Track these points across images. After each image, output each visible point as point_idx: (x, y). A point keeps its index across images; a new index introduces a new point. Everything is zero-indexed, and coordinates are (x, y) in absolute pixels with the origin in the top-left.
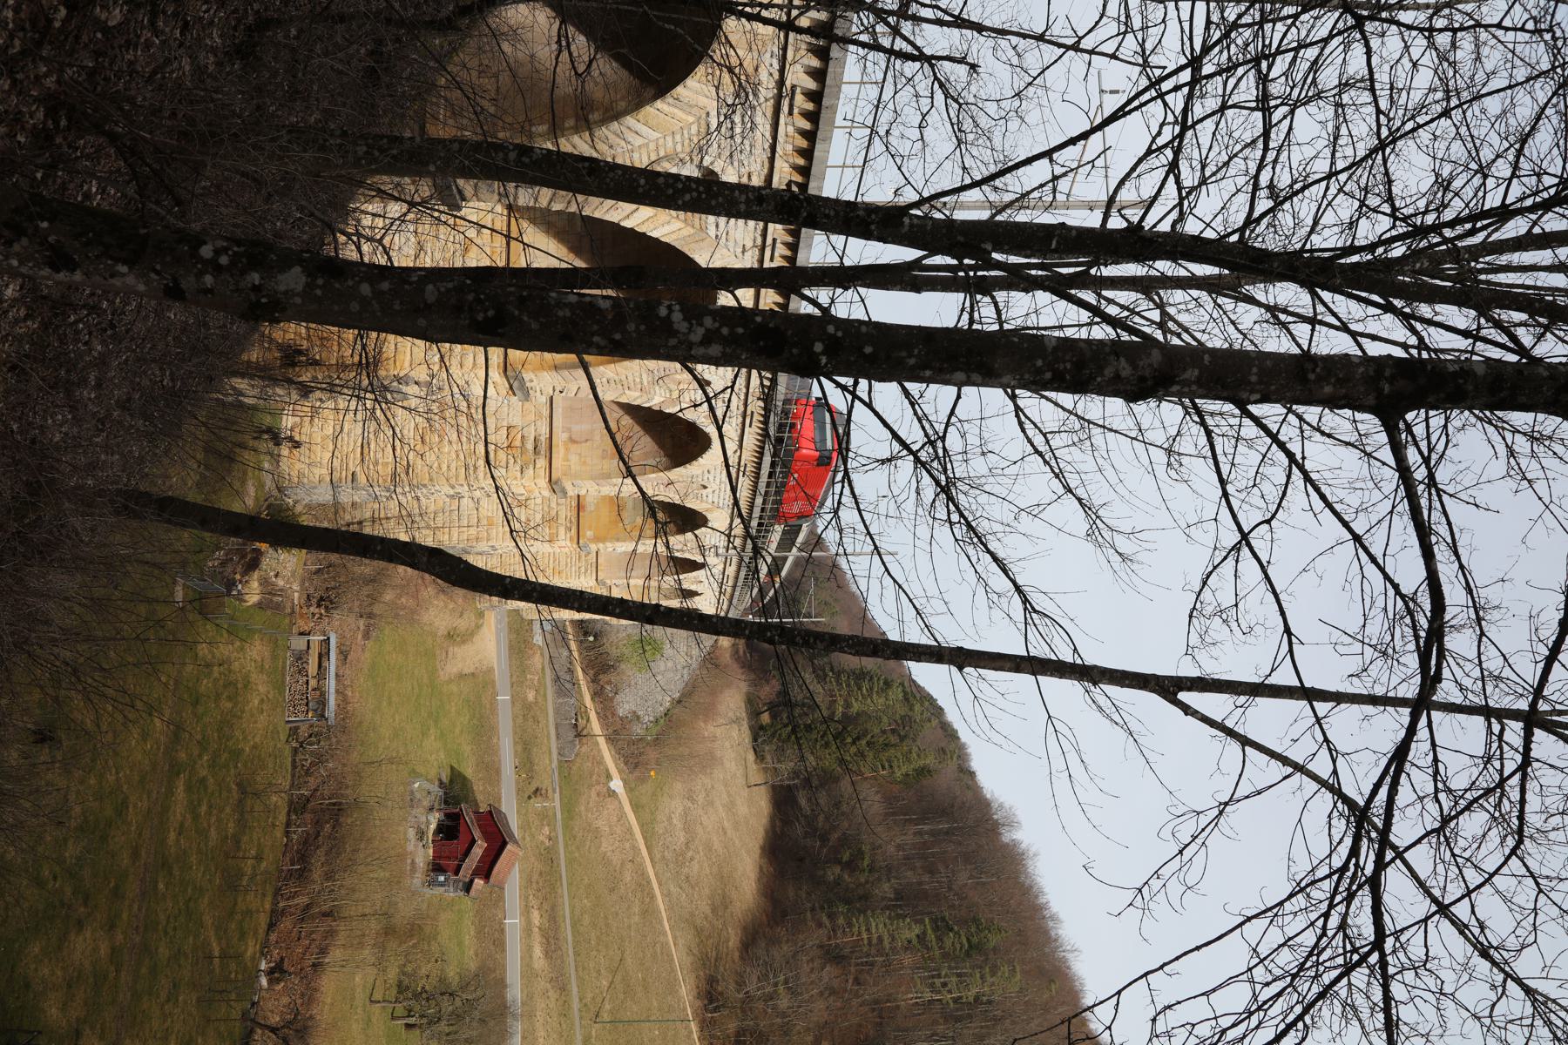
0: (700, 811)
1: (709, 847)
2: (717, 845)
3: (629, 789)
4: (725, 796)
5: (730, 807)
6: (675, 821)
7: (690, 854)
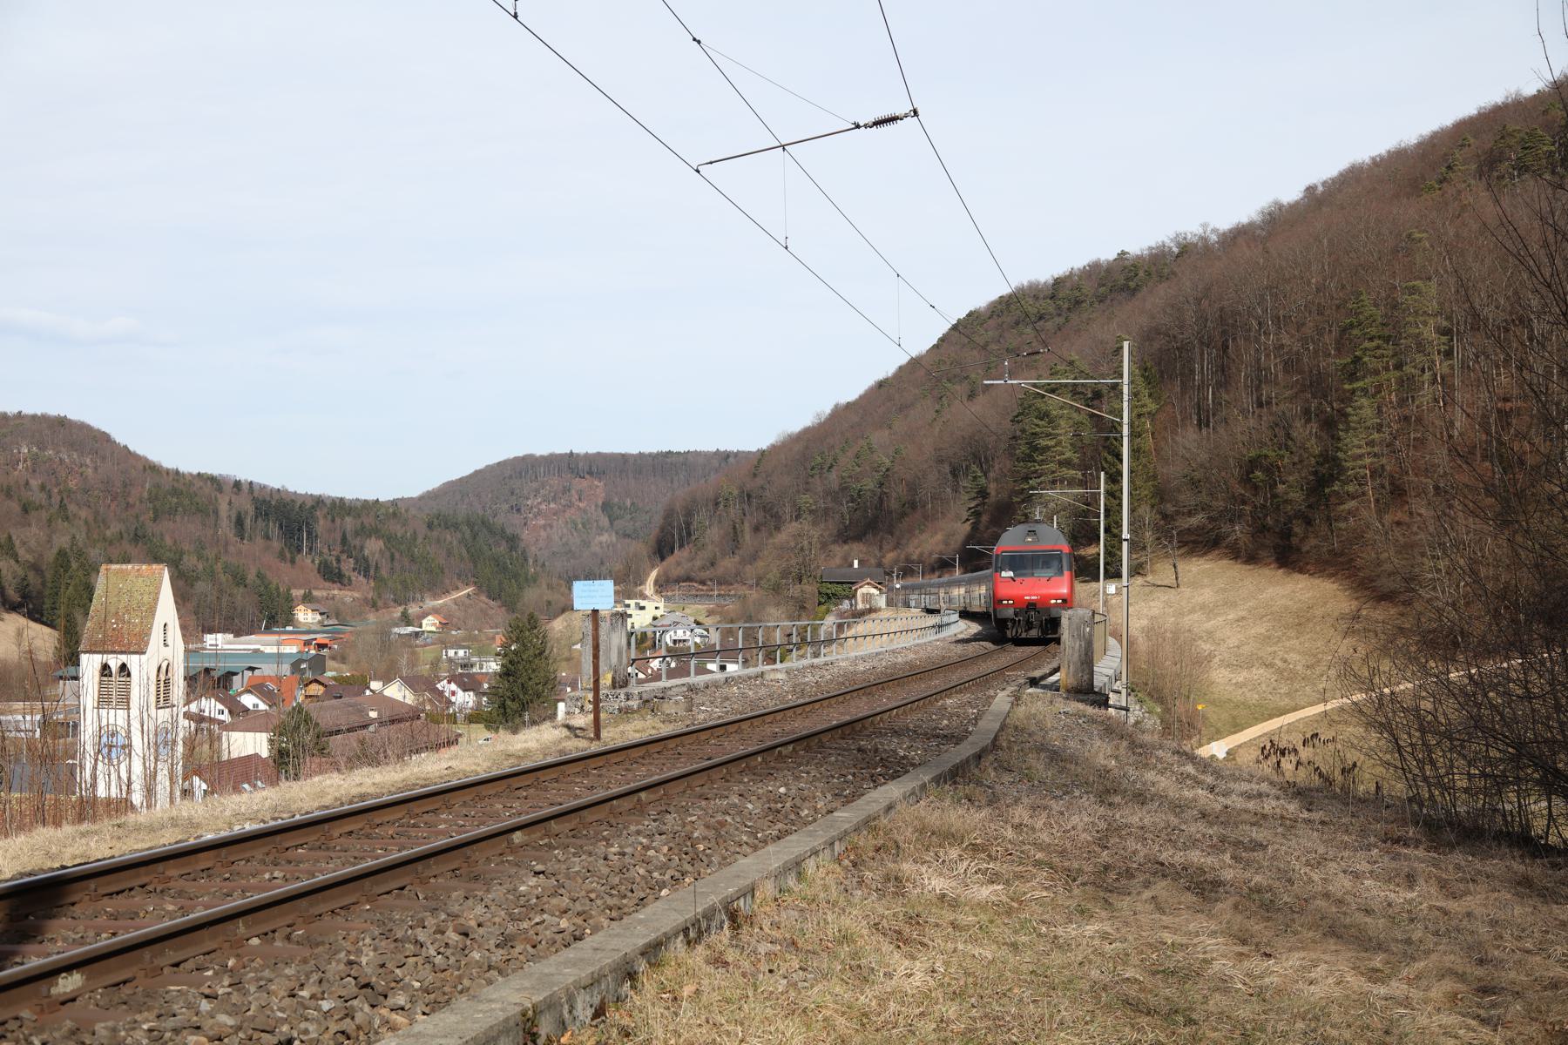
0: (1223, 648)
1: (1266, 639)
2: (1261, 629)
3: (1218, 735)
4: (1195, 617)
5: (1209, 611)
6: (1241, 679)
7: (1279, 663)
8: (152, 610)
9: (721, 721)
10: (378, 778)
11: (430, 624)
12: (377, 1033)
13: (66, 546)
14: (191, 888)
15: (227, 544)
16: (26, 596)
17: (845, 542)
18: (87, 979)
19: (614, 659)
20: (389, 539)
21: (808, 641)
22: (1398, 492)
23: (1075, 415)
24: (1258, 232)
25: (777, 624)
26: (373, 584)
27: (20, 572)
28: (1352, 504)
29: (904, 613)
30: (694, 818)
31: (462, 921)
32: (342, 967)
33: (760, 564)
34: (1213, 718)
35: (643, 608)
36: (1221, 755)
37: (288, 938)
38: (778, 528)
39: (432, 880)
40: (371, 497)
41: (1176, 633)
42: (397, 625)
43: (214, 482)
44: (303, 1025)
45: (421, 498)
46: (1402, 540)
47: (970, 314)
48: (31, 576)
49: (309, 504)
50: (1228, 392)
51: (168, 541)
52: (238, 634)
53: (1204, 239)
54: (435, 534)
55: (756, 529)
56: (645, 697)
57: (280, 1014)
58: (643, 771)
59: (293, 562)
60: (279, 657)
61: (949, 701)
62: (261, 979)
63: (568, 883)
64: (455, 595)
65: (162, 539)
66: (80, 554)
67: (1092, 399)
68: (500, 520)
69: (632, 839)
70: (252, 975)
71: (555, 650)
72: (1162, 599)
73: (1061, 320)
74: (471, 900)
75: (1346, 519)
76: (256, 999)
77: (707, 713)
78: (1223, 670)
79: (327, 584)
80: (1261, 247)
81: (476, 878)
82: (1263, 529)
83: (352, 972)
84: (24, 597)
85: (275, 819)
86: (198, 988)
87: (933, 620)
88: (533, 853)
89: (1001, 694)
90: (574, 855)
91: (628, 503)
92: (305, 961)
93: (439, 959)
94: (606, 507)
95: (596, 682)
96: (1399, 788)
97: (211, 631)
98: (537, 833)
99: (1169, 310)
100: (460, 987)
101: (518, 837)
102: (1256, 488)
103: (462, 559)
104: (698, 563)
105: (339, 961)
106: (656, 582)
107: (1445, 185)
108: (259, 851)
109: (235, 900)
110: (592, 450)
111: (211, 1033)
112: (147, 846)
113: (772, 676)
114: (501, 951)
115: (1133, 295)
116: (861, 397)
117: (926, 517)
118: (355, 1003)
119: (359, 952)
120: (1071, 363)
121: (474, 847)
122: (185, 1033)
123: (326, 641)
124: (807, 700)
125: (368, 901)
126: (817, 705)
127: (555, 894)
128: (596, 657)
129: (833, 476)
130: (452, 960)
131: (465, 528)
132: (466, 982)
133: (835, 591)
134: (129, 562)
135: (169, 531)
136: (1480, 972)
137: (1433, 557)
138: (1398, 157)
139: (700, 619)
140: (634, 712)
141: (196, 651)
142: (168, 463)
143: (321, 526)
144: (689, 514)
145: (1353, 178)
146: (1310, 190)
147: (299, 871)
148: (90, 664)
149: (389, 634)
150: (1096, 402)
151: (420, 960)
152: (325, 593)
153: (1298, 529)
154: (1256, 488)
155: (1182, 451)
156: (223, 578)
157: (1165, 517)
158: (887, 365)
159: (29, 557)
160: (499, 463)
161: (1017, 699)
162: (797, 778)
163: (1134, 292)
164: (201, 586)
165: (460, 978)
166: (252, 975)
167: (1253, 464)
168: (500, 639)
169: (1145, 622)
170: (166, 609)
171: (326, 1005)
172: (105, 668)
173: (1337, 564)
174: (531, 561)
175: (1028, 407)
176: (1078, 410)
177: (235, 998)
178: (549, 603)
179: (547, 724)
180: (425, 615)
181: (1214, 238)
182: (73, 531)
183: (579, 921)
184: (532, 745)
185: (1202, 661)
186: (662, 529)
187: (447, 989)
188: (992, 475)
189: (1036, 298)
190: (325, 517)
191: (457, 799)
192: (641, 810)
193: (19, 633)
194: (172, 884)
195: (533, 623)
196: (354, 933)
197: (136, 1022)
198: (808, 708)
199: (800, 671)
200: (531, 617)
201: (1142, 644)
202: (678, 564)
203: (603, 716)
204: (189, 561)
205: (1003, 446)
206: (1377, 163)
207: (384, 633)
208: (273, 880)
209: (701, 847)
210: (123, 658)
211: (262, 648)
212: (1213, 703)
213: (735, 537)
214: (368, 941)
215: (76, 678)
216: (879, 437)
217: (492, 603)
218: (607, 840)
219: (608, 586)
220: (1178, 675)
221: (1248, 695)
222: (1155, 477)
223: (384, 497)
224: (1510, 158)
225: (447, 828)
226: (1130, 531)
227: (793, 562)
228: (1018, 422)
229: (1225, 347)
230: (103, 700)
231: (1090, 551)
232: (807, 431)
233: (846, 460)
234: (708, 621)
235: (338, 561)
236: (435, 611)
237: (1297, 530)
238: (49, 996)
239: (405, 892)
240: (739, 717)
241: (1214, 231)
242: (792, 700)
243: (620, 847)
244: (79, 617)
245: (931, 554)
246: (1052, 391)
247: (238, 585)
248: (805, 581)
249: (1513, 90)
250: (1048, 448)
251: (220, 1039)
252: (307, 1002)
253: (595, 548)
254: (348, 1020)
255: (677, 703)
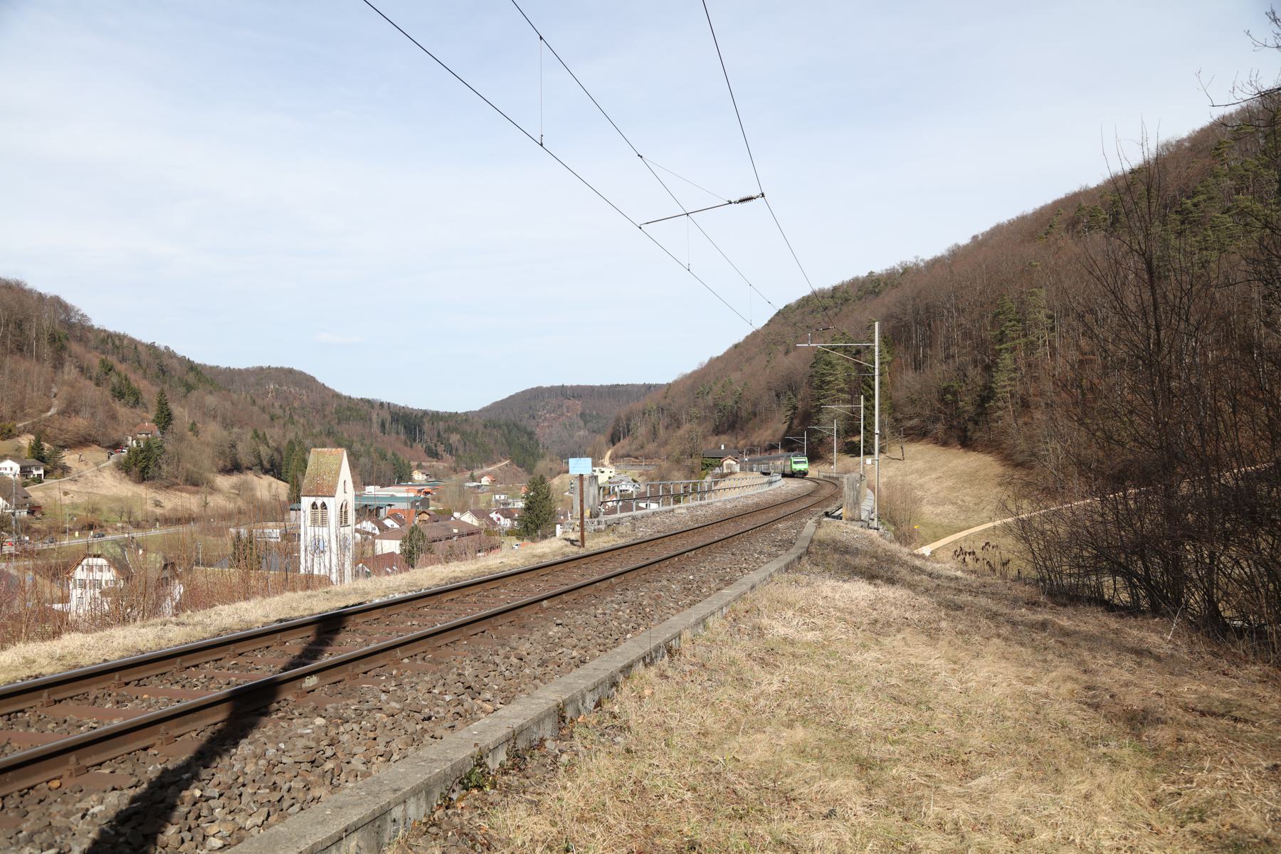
0: (929, 493)
1: (953, 489)
2: (950, 483)
6: (939, 511)
7: (960, 502)
8: (338, 473)
9: (652, 538)
10: (463, 568)
11: (485, 481)
12: (476, 714)
13: (293, 438)
14: (369, 629)
15: (376, 437)
16: (272, 464)
17: (716, 435)
18: (320, 680)
19: (591, 502)
20: (463, 434)
21: (696, 491)
22: (1025, 405)
23: (846, 363)
24: (946, 261)
25: (678, 482)
26: (454, 459)
27: (270, 453)
28: (1000, 413)
29: (750, 475)
30: (643, 594)
31: (519, 651)
32: (455, 676)
33: (669, 447)
34: (923, 533)
35: (603, 472)
36: (927, 554)
37: (424, 659)
38: (678, 427)
39: (500, 628)
40: (453, 410)
41: (903, 486)
42: (468, 482)
43: (370, 403)
44: (436, 709)
45: (480, 411)
46: (1028, 433)
47: (786, 307)
48: (276, 456)
49: (420, 415)
50: (931, 350)
51: (346, 435)
52: (382, 486)
53: (916, 265)
54: (488, 431)
55: (667, 428)
56: (608, 523)
57: (423, 703)
58: (610, 566)
59: (411, 447)
60: (408, 499)
61: (780, 526)
62: (412, 682)
63: (575, 630)
64: (500, 465)
65: (342, 434)
66: (300, 442)
67: (855, 354)
68: (524, 423)
69: (609, 605)
70: (407, 680)
71: (555, 496)
72: (895, 466)
73: (837, 310)
74: (522, 640)
75: (997, 422)
76: (411, 694)
77: (644, 532)
78: (929, 506)
79: (430, 459)
80: (948, 269)
81: (523, 627)
82: (951, 427)
83: (461, 680)
84: (272, 465)
85: (411, 591)
86: (378, 686)
87: (766, 479)
88: (554, 612)
89: (810, 522)
90: (577, 614)
91: (595, 413)
92: (434, 673)
93: (507, 673)
94: (582, 415)
95: (582, 515)
96: (1034, 574)
97: (369, 484)
98: (556, 601)
99: (898, 305)
100: (519, 689)
101: (545, 603)
102: (946, 404)
103: (503, 445)
104: (634, 447)
105: (453, 673)
106: (610, 457)
107: (1049, 236)
108: (404, 609)
109: (393, 638)
110: (575, 384)
111: (388, 712)
112: (343, 605)
113: (679, 511)
114: (541, 669)
115: (877, 296)
116: (725, 353)
117: (762, 421)
118: (463, 696)
119: (464, 668)
120: (844, 334)
121: (522, 609)
122: (374, 711)
123: (430, 490)
124: (700, 525)
125: (465, 639)
126: (706, 528)
127: (568, 637)
128: (582, 501)
129: (710, 397)
130: (514, 674)
131: (504, 428)
132: (523, 686)
133: (711, 462)
134: (325, 447)
135: (345, 430)
136: (1085, 677)
137: (1045, 442)
138: (1022, 220)
139: (635, 478)
140: (602, 531)
141: (360, 496)
142: (345, 391)
143: (426, 427)
144: (629, 419)
145: (998, 231)
146: (975, 238)
147: (427, 621)
148: (306, 502)
149: (463, 486)
150: (857, 356)
151: (497, 673)
152: (428, 464)
153: (970, 426)
154: (946, 404)
155: (905, 383)
156: (374, 455)
157: (896, 420)
158: (740, 333)
159: (274, 444)
160: (523, 392)
161: (819, 524)
162: (699, 570)
163: (877, 294)
164: (363, 460)
165: (519, 684)
166: (407, 680)
167: (946, 390)
168: (524, 489)
169: (885, 480)
170: (346, 473)
171: (448, 698)
172: (314, 506)
173: (992, 446)
174: (541, 446)
175: (819, 358)
176: (848, 360)
177: (399, 693)
178: (551, 469)
179: (553, 539)
180: (483, 476)
181: (922, 264)
182: (296, 430)
183: (583, 652)
184: (547, 550)
185: (917, 501)
186: (614, 428)
187: (512, 690)
188: (799, 397)
189: (823, 297)
190: (429, 422)
191: (510, 581)
192: (612, 588)
193: (270, 485)
194: (359, 627)
195: (542, 480)
196: (459, 658)
197: (348, 705)
198: (701, 530)
199: (695, 508)
200: (542, 477)
201: (884, 492)
202: (623, 447)
203: (585, 533)
204: (357, 446)
205: (806, 381)
206: (1011, 223)
207: (461, 486)
208: (411, 626)
209: (648, 610)
210: (325, 500)
211: (395, 494)
212: (923, 525)
213: (654, 433)
214: (468, 662)
215: (300, 510)
216: (735, 376)
217: (520, 469)
218: (594, 605)
219: (588, 461)
220: (904, 510)
221: (943, 520)
222: (890, 398)
223: (460, 411)
224: (1083, 222)
225: (505, 597)
226: (880, 429)
227: (687, 446)
228: (814, 367)
229: (929, 325)
230: (314, 522)
231: (856, 439)
232: (694, 373)
233: (717, 389)
234: (640, 480)
235: (436, 446)
236: (488, 474)
237: (969, 427)
238: (301, 688)
239: (485, 634)
240: (662, 535)
241: (922, 260)
242: (692, 525)
243: (603, 610)
244: (300, 477)
245: (765, 442)
246: (833, 350)
247: (383, 459)
248: (694, 457)
249: (1084, 184)
250: (830, 382)
251: (393, 716)
252: (438, 696)
253: (576, 439)
254: (460, 706)
255: (626, 526)
